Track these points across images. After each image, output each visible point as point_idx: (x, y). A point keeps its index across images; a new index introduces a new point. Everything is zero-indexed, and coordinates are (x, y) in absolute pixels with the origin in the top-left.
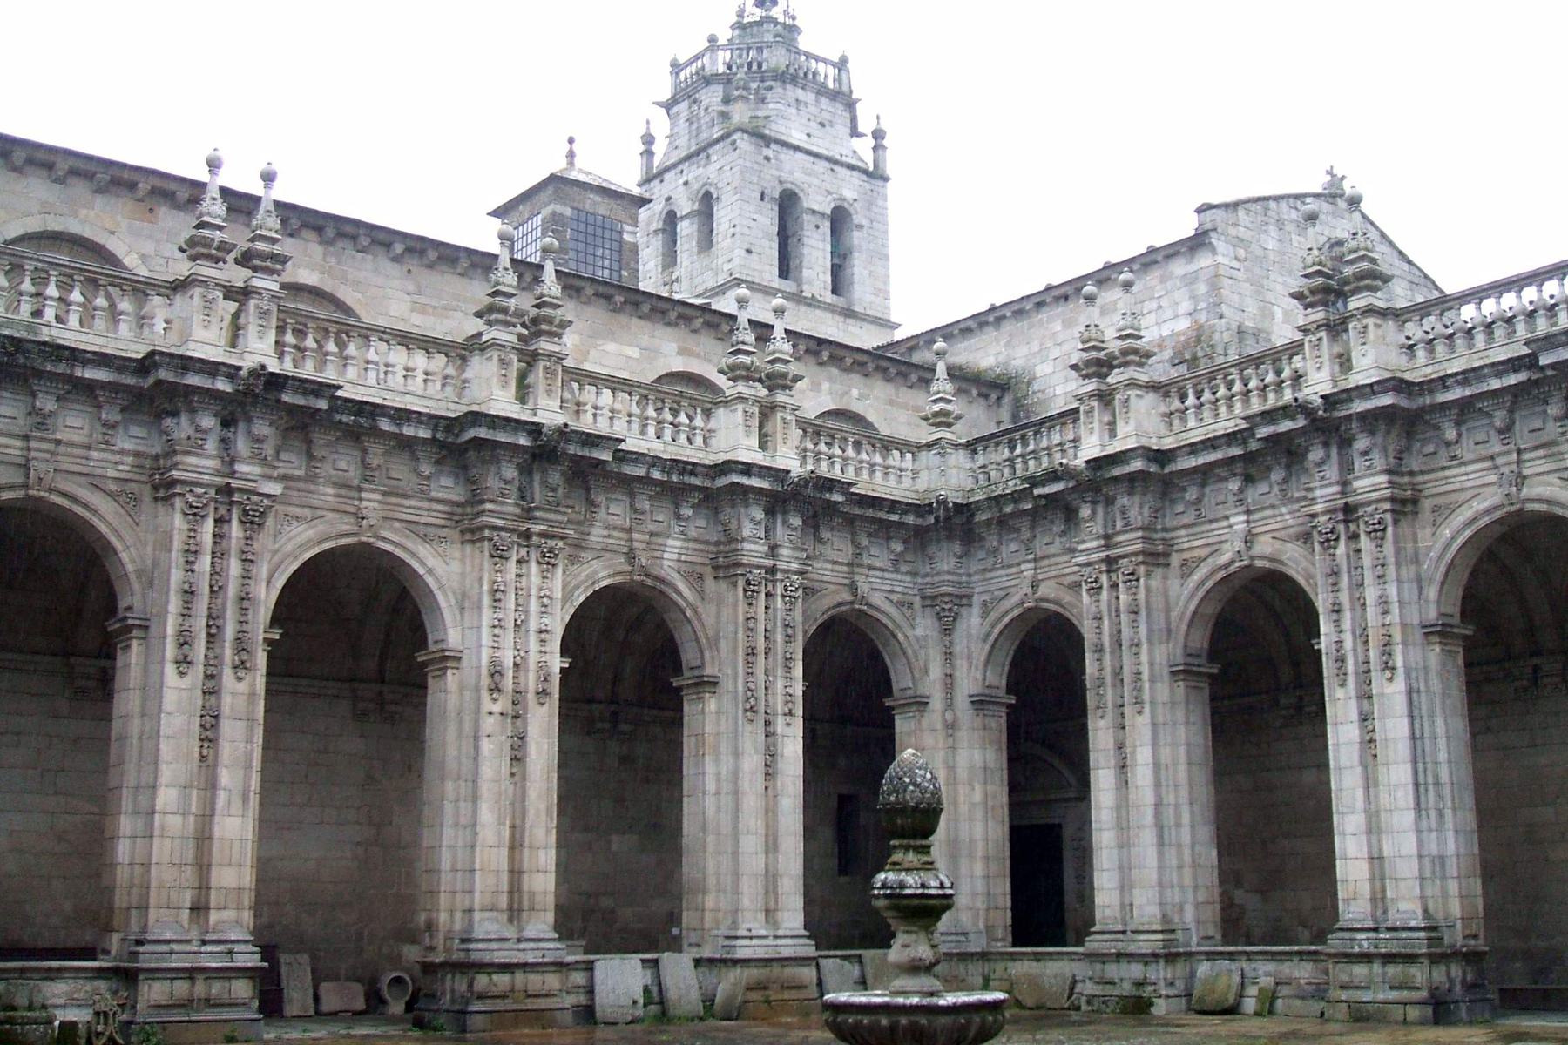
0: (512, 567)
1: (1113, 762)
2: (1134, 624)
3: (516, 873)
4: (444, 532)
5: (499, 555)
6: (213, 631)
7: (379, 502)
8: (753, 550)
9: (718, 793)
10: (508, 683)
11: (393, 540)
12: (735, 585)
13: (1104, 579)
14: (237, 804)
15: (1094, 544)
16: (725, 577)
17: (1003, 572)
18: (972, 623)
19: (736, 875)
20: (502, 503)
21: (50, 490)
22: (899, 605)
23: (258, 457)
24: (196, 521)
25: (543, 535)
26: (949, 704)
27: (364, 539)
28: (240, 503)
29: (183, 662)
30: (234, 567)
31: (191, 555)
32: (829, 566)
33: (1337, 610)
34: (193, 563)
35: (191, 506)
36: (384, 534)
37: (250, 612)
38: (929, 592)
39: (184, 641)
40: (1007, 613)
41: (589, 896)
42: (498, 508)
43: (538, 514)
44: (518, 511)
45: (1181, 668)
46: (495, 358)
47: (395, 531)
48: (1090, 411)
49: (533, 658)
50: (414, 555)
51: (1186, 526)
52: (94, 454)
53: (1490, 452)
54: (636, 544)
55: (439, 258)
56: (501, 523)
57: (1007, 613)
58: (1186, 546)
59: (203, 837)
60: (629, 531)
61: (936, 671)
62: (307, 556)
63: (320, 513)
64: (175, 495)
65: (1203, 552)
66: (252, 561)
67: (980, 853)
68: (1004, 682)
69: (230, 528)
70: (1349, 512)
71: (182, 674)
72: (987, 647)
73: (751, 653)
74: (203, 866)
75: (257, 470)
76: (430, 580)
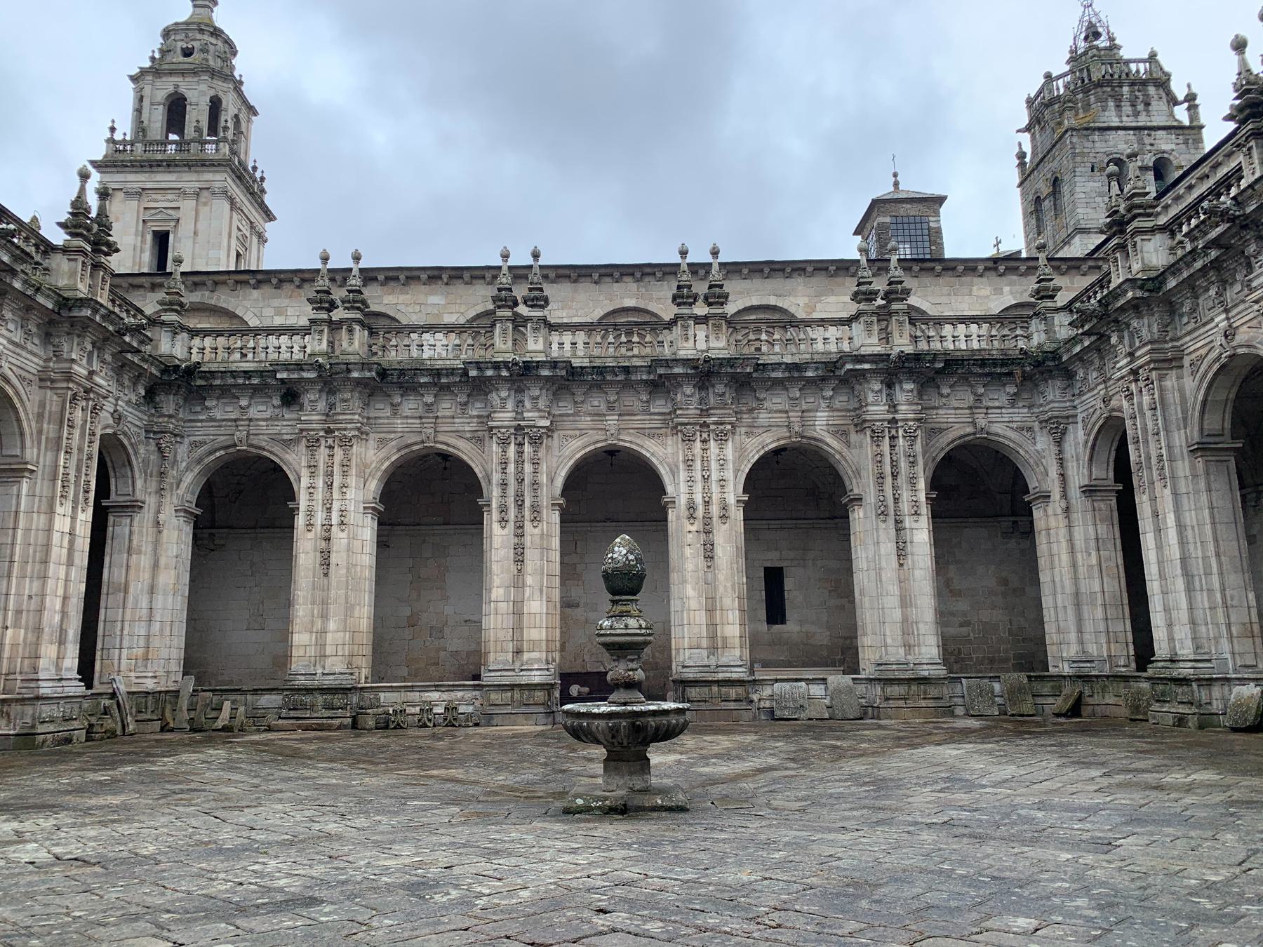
0: (698, 444)
3: (712, 626)
4: (663, 431)
5: (688, 439)
10: (700, 512)
11: (629, 440)
13: (1133, 387)
14: (537, 593)
17: (1090, 395)
21: (435, 442)
23: (535, 408)
25: (715, 423)
26: (1065, 495)
29: (503, 521)
30: (528, 468)
31: (504, 464)
32: (953, 412)
36: (622, 438)
39: (503, 510)
40: (1094, 424)
41: (846, 638)
44: (699, 412)
45: (1196, 447)
47: (630, 434)
49: (716, 497)
51: (1189, 333)
52: (457, 420)
56: (686, 420)
58: (1192, 349)
59: (518, 613)
60: (787, 412)
62: (578, 456)
65: (1203, 351)
68: (1111, 474)
71: (503, 528)
72: (1088, 451)
73: (881, 476)
74: (518, 628)
75: (536, 414)
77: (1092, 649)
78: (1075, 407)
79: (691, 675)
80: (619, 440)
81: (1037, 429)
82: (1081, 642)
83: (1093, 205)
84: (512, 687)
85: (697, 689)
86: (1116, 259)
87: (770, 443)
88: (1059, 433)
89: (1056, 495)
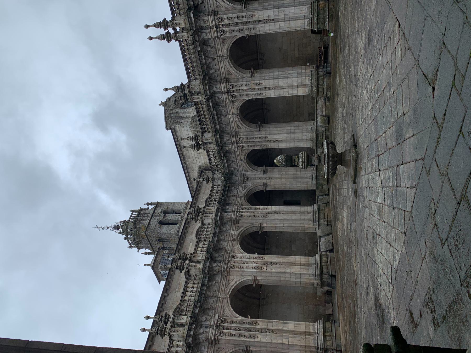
0: (235, 264)
1: (277, 143)
3: (301, 265)
4: (228, 279)
5: (233, 267)
6: (248, 330)
7: (221, 293)
8: (233, 215)
9: (283, 224)
10: (260, 265)
11: (229, 291)
12: (240, 219)
13: (240, 145)
14: (287, 325)
15: (233, 146)
17: (239, 167)
18: (250, 174)
19: (300, 220)
20: (222, 266)
22: (245, 188)
23: (210, 320)
24: (224, 334)
26: (265, 178)
27: (229, 297)
28: (220, 323)
29: (255, 337)
31: (231, 335)
32: (237, 201)
33: (248, 95)
34: (233, 334)
35: (220, 335)
37: (244, 321)
38: (242, 182)
39: (250, 337)
40: (247, 166)
42: (223, 267)
43: (224, 259)
44: (223, 263)
46: (191, 268)
47: (227, 290)
49: (255, 260)
50: (232, 286)
51: (231, 128)
53: (217, 62)
54: (231, 239)
55: (168, 285)
57: (247, 166)
58: (234, 128)
59: (294, 333)
60: (228, 240)
61: (258, 181)
62: (232, 310)
63: (223, 307)
64: (217, 339)
65: (236, 124)
66: (233, 321)
67: (296, 173)
68: (261, 168)
69: (225, 326)
70: (228, 92)
71: (257, 337)
72: (254, 170)
73: (254, 216)
74: (301, 333)
75: (213, 319)
76: (238, 283)
77: (309, 175)
78: (241, 174)
79: (319, 271)
80: (228, 294)
81: (245, 185)
82: (307, 178)
83: (171, 229)
84: (325, 336)
85: (323, 270)
86: (206, 147)
87: (238, 246)
88: (249, 179)
89: (265, 181)
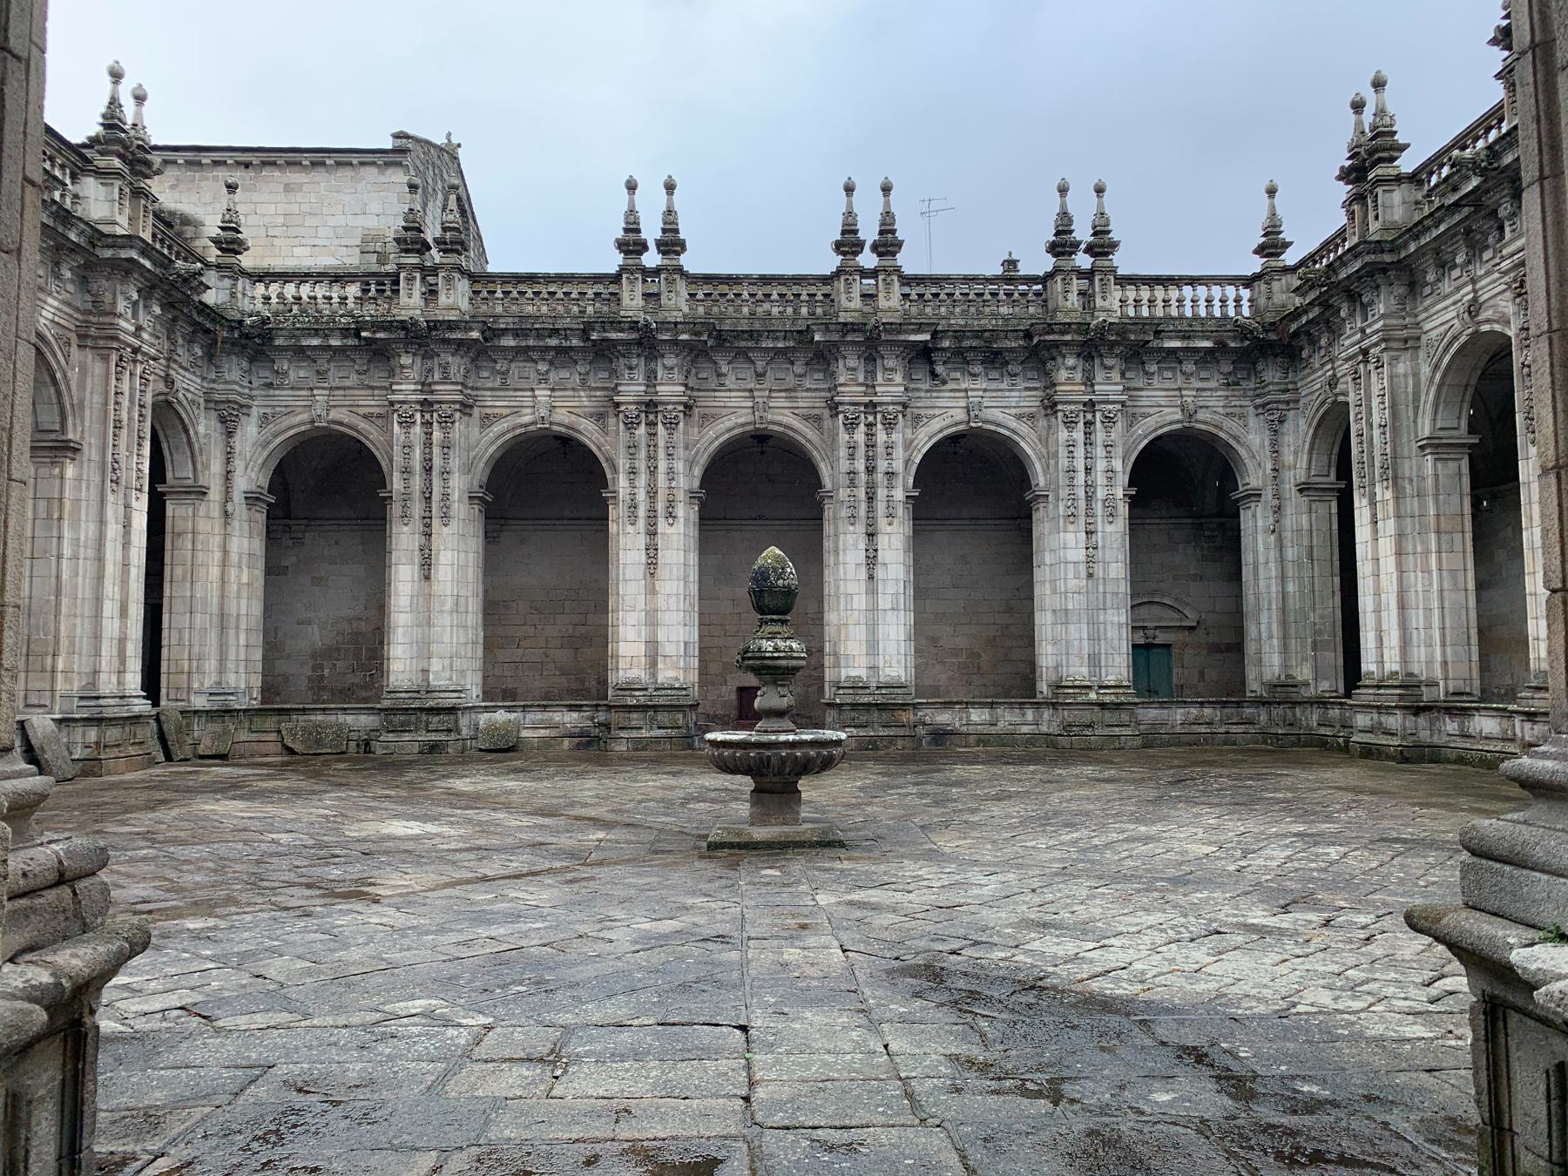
1: (416, 560)
2: (445, 456)
9: (75, 558)
12: (106, 359)
15: (412, 387)
16: (92, 348)
17: (291, 393)
18: (249, 432)
19: (97, 637)
33: (633, 472)
38: (217, 397)
40: (292, 427)
48: (410, 280)
53: (749, 387)
57: (292, 427)
61: (216, 467)
65: (505, 411)
67: (243, 626)
70: (651, 406)
72: (266, 453)
78: (251, 397)
81: (202, 407)
82: (222, 670)
86: (414, 278)
89: (215, 494)
